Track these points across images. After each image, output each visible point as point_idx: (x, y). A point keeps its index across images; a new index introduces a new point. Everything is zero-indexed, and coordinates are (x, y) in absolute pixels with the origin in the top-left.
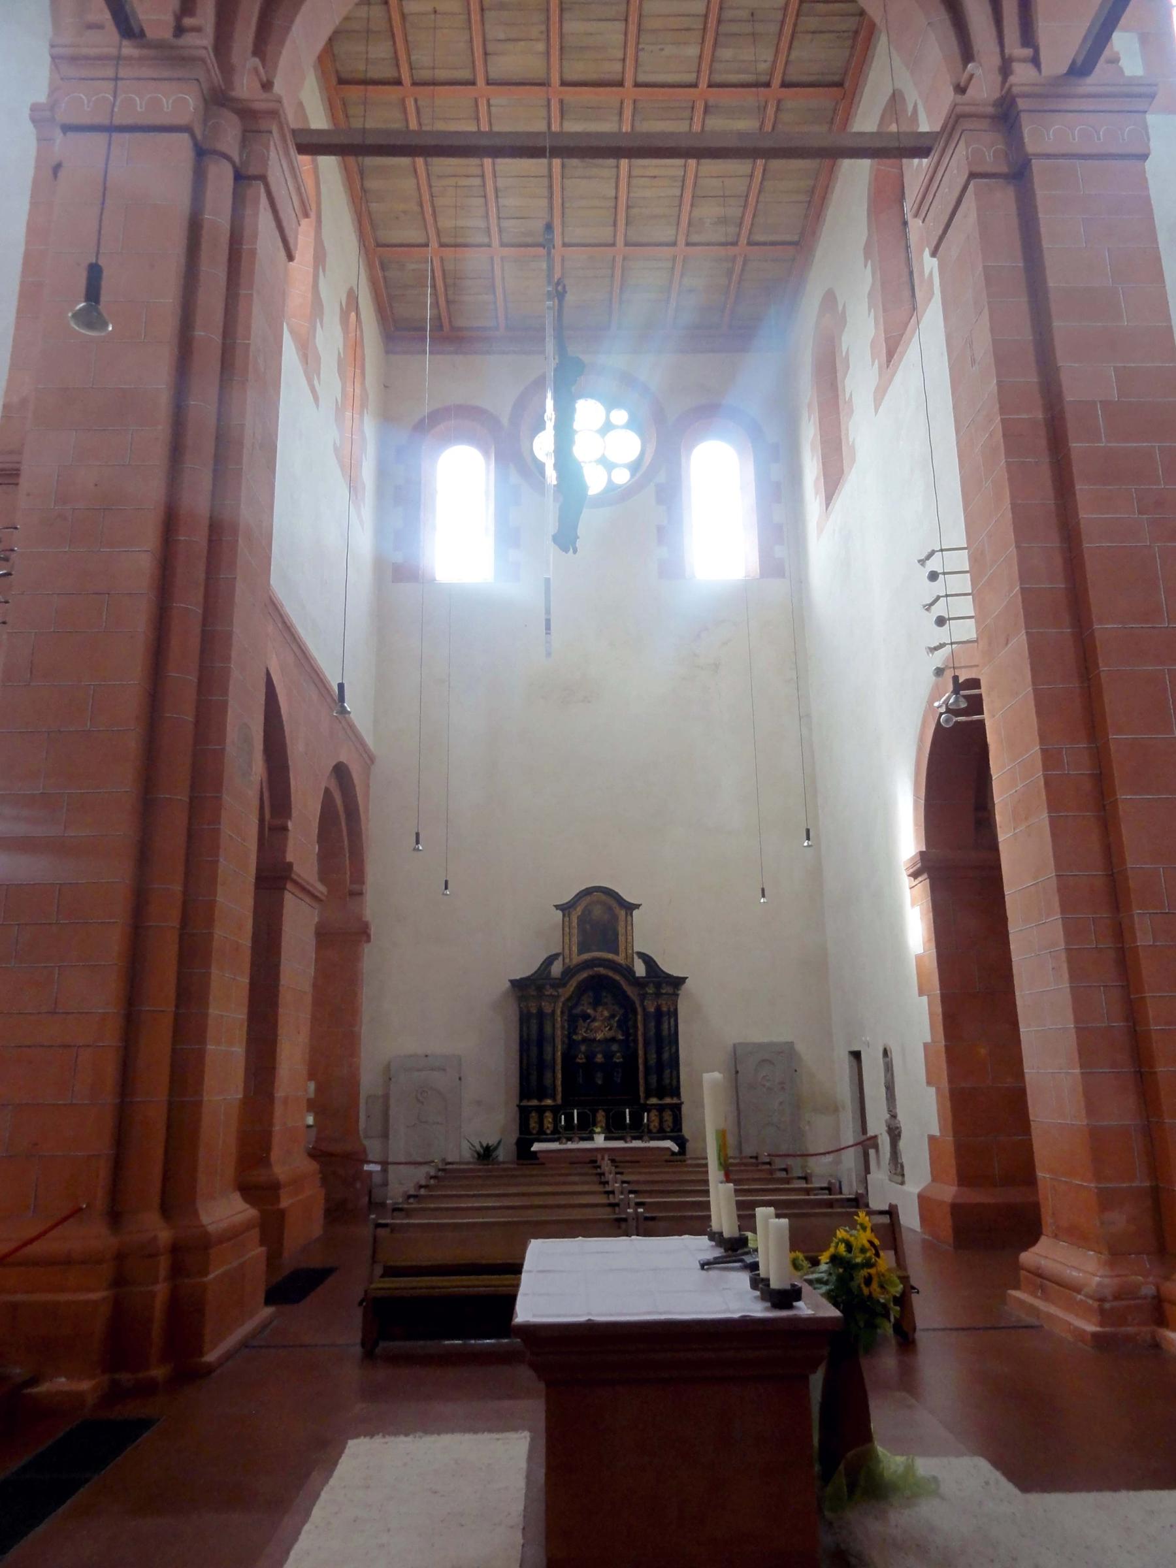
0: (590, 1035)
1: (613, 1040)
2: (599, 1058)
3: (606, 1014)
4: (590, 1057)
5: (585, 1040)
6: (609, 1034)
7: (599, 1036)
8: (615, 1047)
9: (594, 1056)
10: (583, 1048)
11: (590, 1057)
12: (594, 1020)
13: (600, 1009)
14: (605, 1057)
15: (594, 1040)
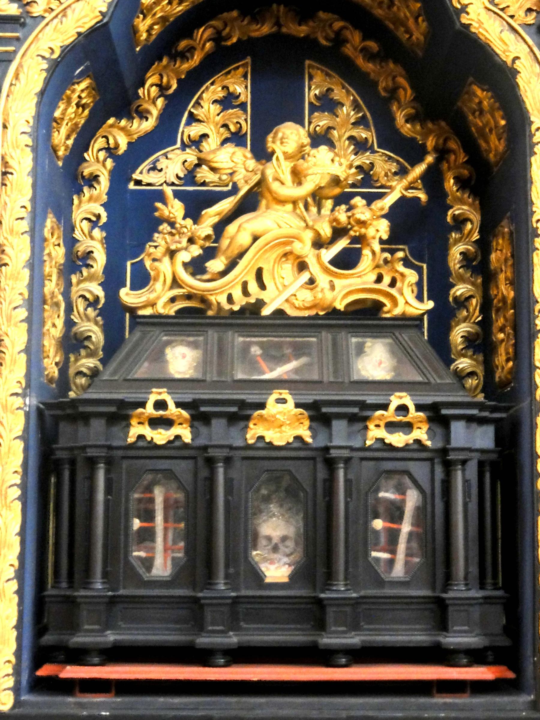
0: (225, 292)
1: (365, 316)
2: (281, 423)
3: (327, 165)
4: (221, 408)
5: (194, 317)
6: (342, 291)
7: (285, 293)
8: (375, 361)
9: (241, 413)
10: (181, 360)
11: (221, 408)
12: (249, 204)
13: (289, 136)
14: (319, 415)
15: (249, 317)
